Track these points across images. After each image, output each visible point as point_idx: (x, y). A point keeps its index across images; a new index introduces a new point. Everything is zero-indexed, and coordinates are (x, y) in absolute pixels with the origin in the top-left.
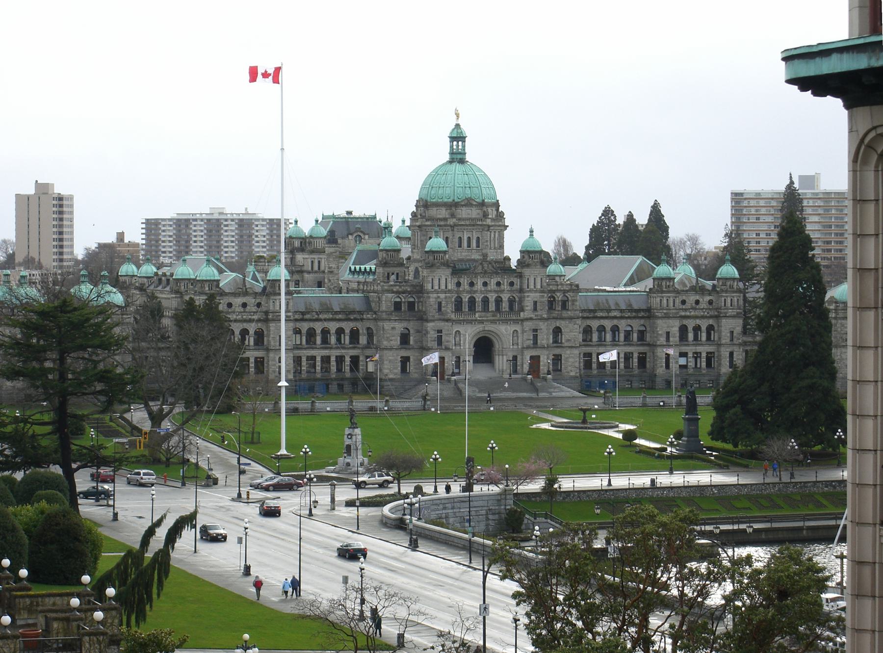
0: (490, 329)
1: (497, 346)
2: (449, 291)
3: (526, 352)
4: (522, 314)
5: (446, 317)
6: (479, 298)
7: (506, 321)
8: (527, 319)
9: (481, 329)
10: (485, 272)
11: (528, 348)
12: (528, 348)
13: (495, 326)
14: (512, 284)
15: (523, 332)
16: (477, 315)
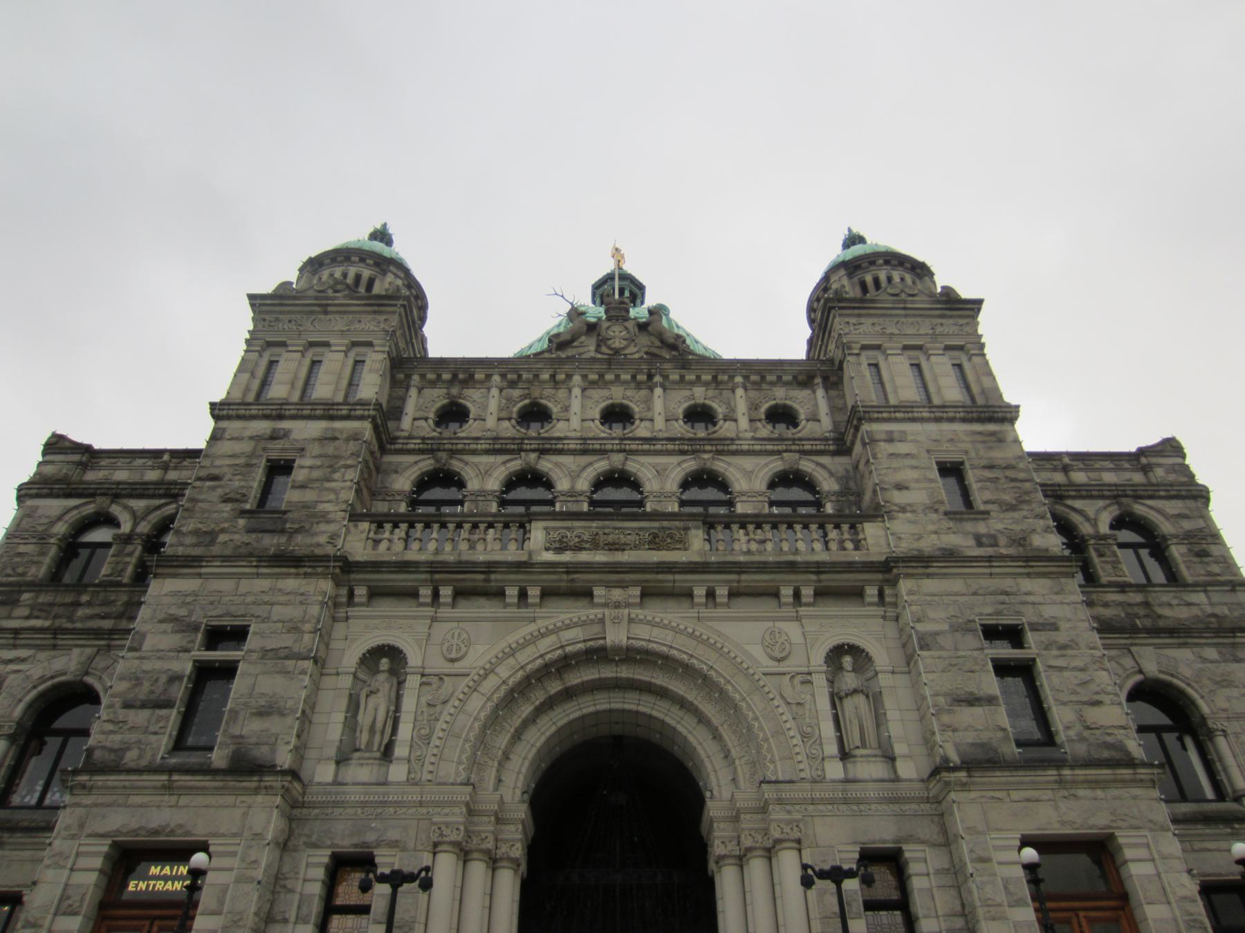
0: (642, 632)
1: (724, 789)
2: (363, 403)
3: (969, 808)
4: (871, 531)
5: (300, 544)
6: (571, 477)
7: (752, 585)
8: (921, 562)
9: (575, 639)
10: (614, 359)
11: (981, 762)
12: (981, 762)
13: (672, 614)
14: (782, 415)
15: (911, 649)
16: (538, 534)
